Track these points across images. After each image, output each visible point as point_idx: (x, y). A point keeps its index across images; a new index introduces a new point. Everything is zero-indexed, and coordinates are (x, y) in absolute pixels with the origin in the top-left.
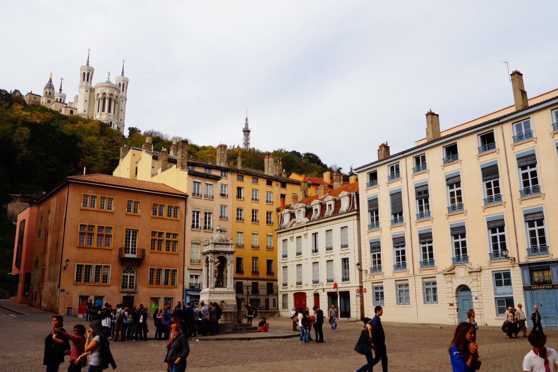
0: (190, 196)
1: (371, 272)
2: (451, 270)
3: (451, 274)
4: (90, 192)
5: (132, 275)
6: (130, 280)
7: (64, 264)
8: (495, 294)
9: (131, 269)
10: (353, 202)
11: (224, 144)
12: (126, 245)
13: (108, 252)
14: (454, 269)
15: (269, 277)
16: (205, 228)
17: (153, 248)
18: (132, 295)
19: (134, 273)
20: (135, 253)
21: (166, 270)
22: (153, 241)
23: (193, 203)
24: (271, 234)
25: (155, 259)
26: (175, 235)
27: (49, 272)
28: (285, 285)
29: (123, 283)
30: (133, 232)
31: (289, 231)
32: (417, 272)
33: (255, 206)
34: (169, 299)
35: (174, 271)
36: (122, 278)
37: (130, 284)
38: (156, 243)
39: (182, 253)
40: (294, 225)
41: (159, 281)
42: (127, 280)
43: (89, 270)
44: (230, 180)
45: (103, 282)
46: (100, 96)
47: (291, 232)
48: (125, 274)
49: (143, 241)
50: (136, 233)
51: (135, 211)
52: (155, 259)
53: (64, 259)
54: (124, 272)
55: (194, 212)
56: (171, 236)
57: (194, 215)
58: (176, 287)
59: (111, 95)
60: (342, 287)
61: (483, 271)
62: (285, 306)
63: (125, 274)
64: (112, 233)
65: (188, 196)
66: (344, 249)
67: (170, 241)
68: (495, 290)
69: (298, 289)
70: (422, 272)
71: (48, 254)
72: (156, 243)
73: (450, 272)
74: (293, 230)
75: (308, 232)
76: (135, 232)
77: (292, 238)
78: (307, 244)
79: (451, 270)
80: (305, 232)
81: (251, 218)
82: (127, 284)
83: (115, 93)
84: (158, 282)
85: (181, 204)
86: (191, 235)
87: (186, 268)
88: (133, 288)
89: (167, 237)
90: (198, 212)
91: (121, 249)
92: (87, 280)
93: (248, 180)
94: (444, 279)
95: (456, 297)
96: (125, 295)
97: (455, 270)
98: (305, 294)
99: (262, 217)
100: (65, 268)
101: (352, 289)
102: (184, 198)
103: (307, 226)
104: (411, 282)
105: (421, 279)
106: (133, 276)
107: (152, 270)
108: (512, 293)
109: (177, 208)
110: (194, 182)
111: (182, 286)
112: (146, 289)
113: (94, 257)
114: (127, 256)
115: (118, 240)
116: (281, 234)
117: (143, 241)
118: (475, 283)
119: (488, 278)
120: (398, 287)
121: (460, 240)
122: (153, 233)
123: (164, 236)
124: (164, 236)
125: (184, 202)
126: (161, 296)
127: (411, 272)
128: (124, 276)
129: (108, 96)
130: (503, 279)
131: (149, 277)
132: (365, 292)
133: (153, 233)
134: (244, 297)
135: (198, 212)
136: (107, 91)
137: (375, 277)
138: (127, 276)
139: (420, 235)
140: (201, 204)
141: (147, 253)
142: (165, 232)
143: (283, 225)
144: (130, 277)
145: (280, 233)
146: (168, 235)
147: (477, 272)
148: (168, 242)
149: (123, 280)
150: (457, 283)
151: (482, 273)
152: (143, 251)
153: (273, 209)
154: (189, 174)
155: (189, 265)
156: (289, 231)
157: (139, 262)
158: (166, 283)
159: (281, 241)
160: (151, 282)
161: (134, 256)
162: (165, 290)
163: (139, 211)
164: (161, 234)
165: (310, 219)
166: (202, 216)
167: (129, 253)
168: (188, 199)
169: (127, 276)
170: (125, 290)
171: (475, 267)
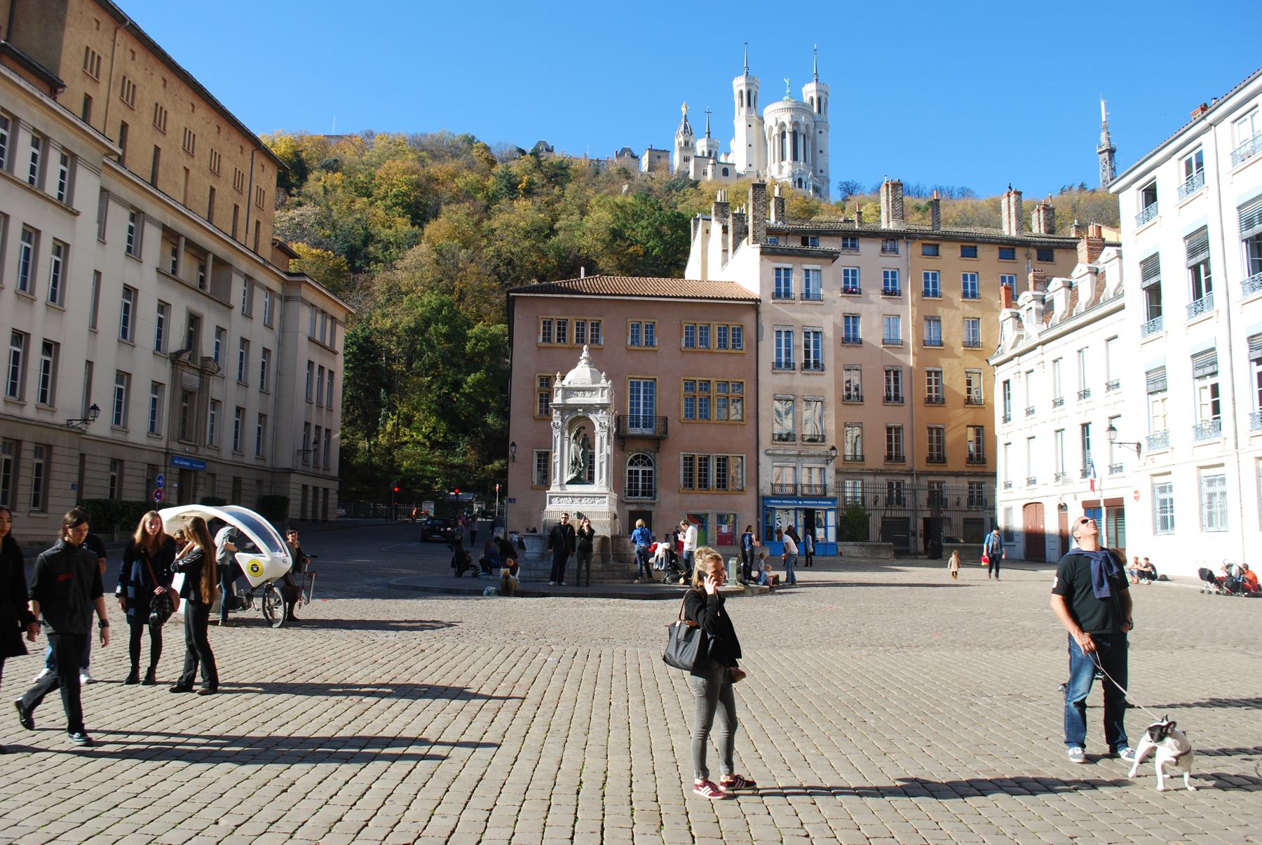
0: (768, 301)
4: (555, 314)
5: (647, 469)
6: (644, 480)
9: (644, 457)
12: (632, 411)
16: (807, 365)
17: (690, 414)
18: (648, 508)
19: (650, 464)
21: (719, 460)
22: (690, 401)
25: (689, 438)
29: (630, 486)
30: (645, 384)
37: (644, 487)
39: (753, 422)
41: (706, 481)
42: (637, 480)
48: (634, 468)
50: (651, 384)
51: (650, 342)
52: (689, 438)
54: (631, 463)
55: (779, 332)
57: (779, 343)
63: (634, 468)
76: (651, 386)
82: (637, 486)
84: (704, 484)
85: (748, 320)
86: (770, 382)
87: (761, 452)
88: (650, 494)
90: (788, 333)
96: (634, 508)
102: (754, 305)
106: (650, 472)
107: (689, 460)
109: (738, 331)
110: (778, 270)
111: (754, 489)
112: (677, 497)
122: (690, 385)
124: (714, 387)
125: (753, 315)
126: (709, 511)
128: (630, 472)
131: (682, 472)
133: (690, 385)
138: (637, 472)
142: (713, 380)
149: (630, 480)
154: (762, 253)
155: (771, 447)
157: (657, 441)
160: (689, 483)
161: (648, 432)
163: (656, 342)
166: (798, 340)
167: (638, 426)
168: (762, 309)
169: (637, 472)
170: (633, 499)
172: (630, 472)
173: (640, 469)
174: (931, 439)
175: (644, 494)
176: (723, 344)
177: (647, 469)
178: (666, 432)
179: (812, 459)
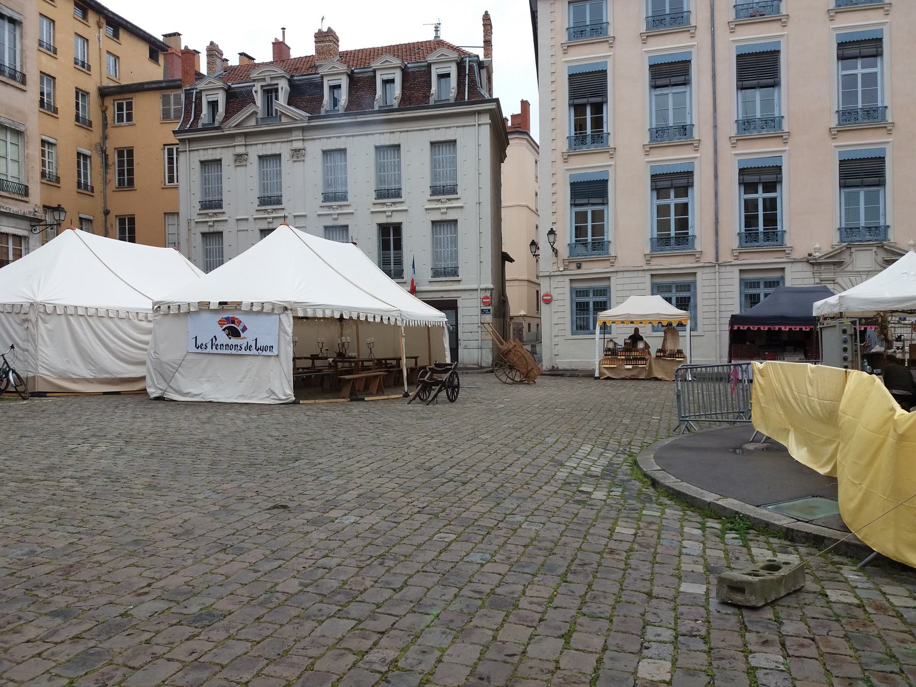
3: (834, 264)
24: (87, 152)
31: (232, 136)
32: (725, 257)
40: (253, 122)
47: (240, 141)
74: (246, 135)
75: (308, 145)
77: (240, 159)
81: (38, 97)
94: (810, 274)
97: (845, 257)
99: (65, 100)
101: (465, 295)
103: (303, 129)
105: (567, 282)
116: (194, 146)
120: (574, 296)
121: (760, 196)
127: (709, 257)
132: (548, 302)
137: (584, 265)
139: (572, 185)
145: (190, 140)
153: (91, 85)
156: (232, 136)
159: (197, 166)
179: (12, 222)
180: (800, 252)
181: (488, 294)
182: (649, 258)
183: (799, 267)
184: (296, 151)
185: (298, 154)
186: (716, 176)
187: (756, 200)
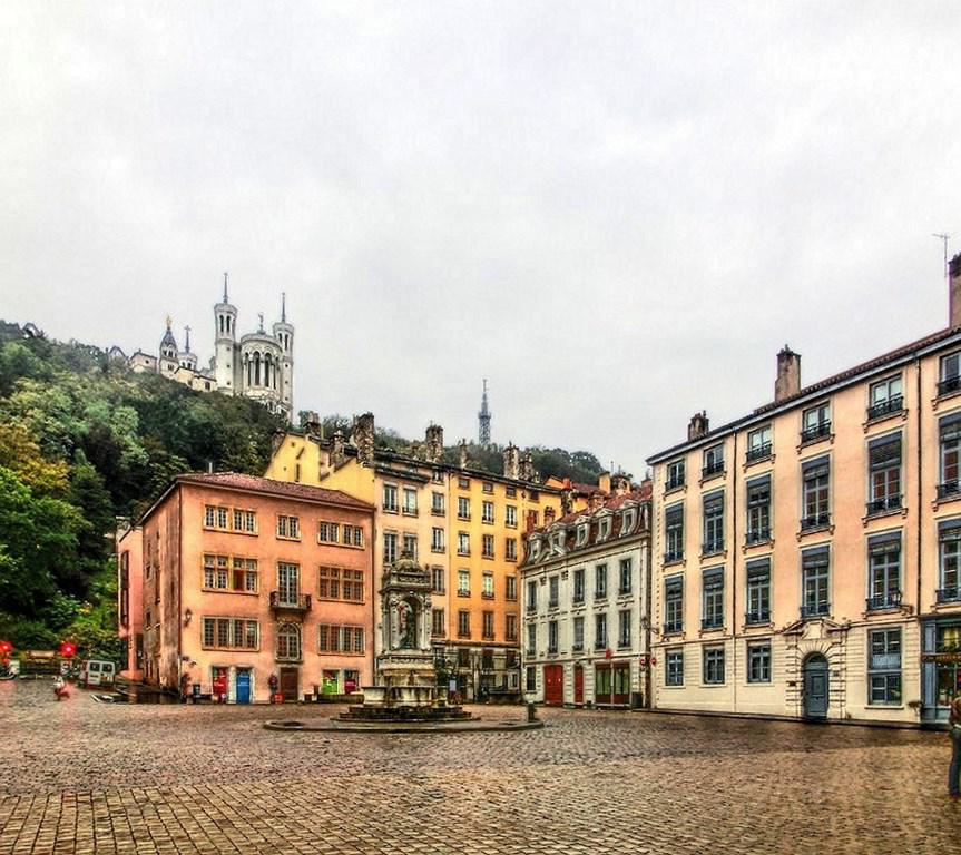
0: (380, 508)
1: (665, 632)
2: (796, 628)
3: (797, 634)
5: (293, 635)
7: (183, 618)
8: (870, 667)
10: (643, 518)
11: (438, 425)
12: (280, 588)
13: (252, 599)
14: (801, 626)
15: (464, 640)
17: (323, 593)
20: (295, 602)
22: (323, 582)
23: (385, 522)
26: (359, 573)
27: (166, 631)
28: (532, 653)
29: (280, 648)
32: (739, 631)
33: (488, 529)
34: (351, 672)
35: (359, 631)
36: (277, 639)
38: (329, 585)
42: (285, 644)
43: (225, 627)
44: (447, 485)
45: (220, 645)
46: (251, 357)
48: (282, 635)
49: (308, 582)
51: (293, 533)
53: (183, 610)
54: (281, 631)
55: (386, 536)
56: (352, 575)
57: (386, 543)
58: (362, 654)
59: (268, 355)
60: (559, 653)
61: (852, 631)
62: (531, 685)
63: (282, 635)
64: (259, 568)
65: (375, 509)
66: (624, 596)
67: (326, 581)
68: (870, 660)
69: (552, 659)
70: (748, 631)
71: (162, 603)
72: (329, 585)
73: (795, 631)
74: (545, 566)
78: (566, 588)
79: (796, 628)
80: (564, 569)
82: (285, 649)
83: (275, 352)
85: (366, 523)
89: (345, 576)
90: (393, 537)
91: (272, 595)
92: (223, 642)
93: (477, 488)
94: (784, 643)
95: (803, 671)
98: (562, 667)
99: (499, 547)
100: (186, 624)
104: (729, 645)
108: (900, 667)
109: (359, 529)
113: (230, 604)
114: (282, 605)
115: (268, 579)
117: (308, 582)
118: (836, 650)
119: (858, 643)
122: (323, 570)
123: (341, 574)
128: (280, 637)
129: (262, 357)
130: (884, 642)
134: (471, 671)
135: (393, 537)
136: (262, 349)
140: (399, 523)
141: (314, 601)
143: (531, 558)
144: (291, 638)
146: (347, 572)
147: (841, 631)
148: (347, 584)
150: (805, 648)
151: (849, 633)
152: (308, 598)
153: (516, 534)
156: (539, 568)
157: (303, 614)
158: (347, 648)
160: (323, 647)
161: (296, 606)
162: (345, 659)
164: (335, 571)
165: (572, 547)
170: (283, 659)
171: (839, 621)
172: (280, 637)
173: (288, 636)
174: (460, 620)
175: (291, 655)
176: (346, 540)
177: (293, 635)
178: (309, 607)
180: (778, 627)
181: (644, 658)
182: (702, 633)
183: (778, 637)
184: (563, 573)
185: (565, 574)
186: (920, 539)
187: (889, 568)
